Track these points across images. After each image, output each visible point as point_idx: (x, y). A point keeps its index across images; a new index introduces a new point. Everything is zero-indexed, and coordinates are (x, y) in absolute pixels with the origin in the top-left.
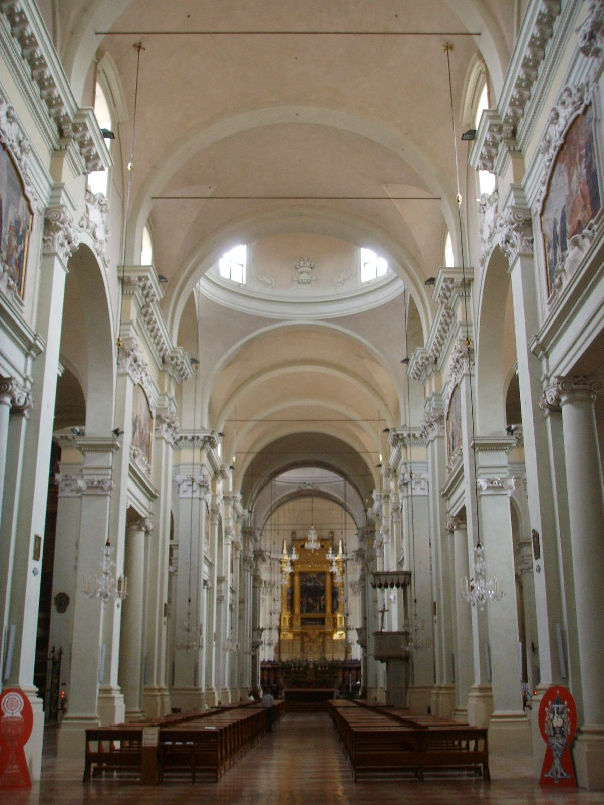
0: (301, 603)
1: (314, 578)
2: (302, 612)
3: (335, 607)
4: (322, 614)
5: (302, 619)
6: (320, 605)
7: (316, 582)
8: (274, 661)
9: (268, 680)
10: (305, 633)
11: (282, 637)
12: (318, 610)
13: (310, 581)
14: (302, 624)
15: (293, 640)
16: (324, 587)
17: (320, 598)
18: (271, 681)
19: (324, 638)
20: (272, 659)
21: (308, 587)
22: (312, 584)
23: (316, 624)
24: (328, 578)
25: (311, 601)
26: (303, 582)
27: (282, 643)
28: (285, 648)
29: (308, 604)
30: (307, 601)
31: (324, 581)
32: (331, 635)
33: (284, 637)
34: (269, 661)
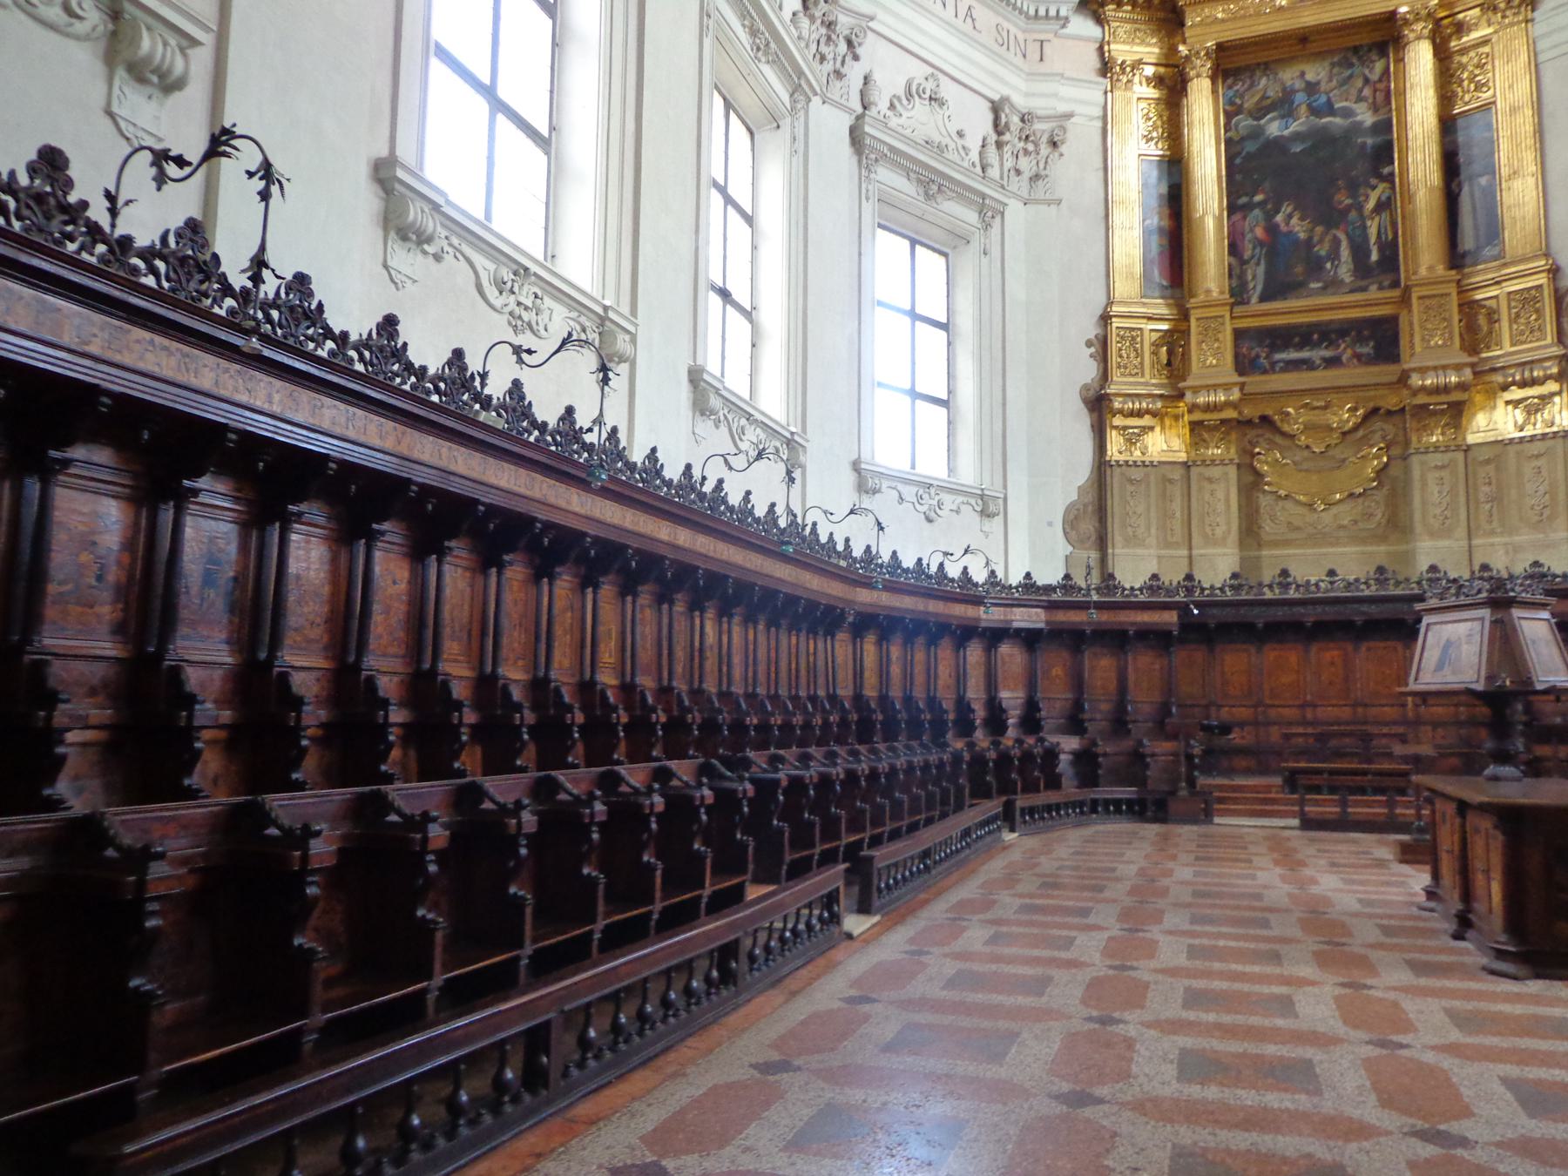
0: (1234, 249)
1: (1311, 88)
2: (1238, 294)
3: (1467, 242)
4: (1373, 293)
5: (1239, 334)
6: (1360, 252)
7: (1330, 109)
8: (1067, 584)
9: (1031, 706)
10: (1265, 420)
11: (1115, 446)
12: (1345, 271)
13: (1283, 105)
14: (1244, 365)
15: (1186, 466)
16: (1384, 127)
17: (1360, 208)
18: (1053, 710)
19: (1399, 450)
20: (1049, 575)
21: (1278, 145)
22: (1295, 127)
23: (1333, 362)
24: (1421, 60)
25: (1298, 227)
26: (1244, 123)
27: (1115, 480)
28: (1128, 507)
29: (1275, 246)
30: (1272, 229)
31: (1387, 97)
32: (1457, 412)
33: (1130, 442)
34: (1028, 585)
